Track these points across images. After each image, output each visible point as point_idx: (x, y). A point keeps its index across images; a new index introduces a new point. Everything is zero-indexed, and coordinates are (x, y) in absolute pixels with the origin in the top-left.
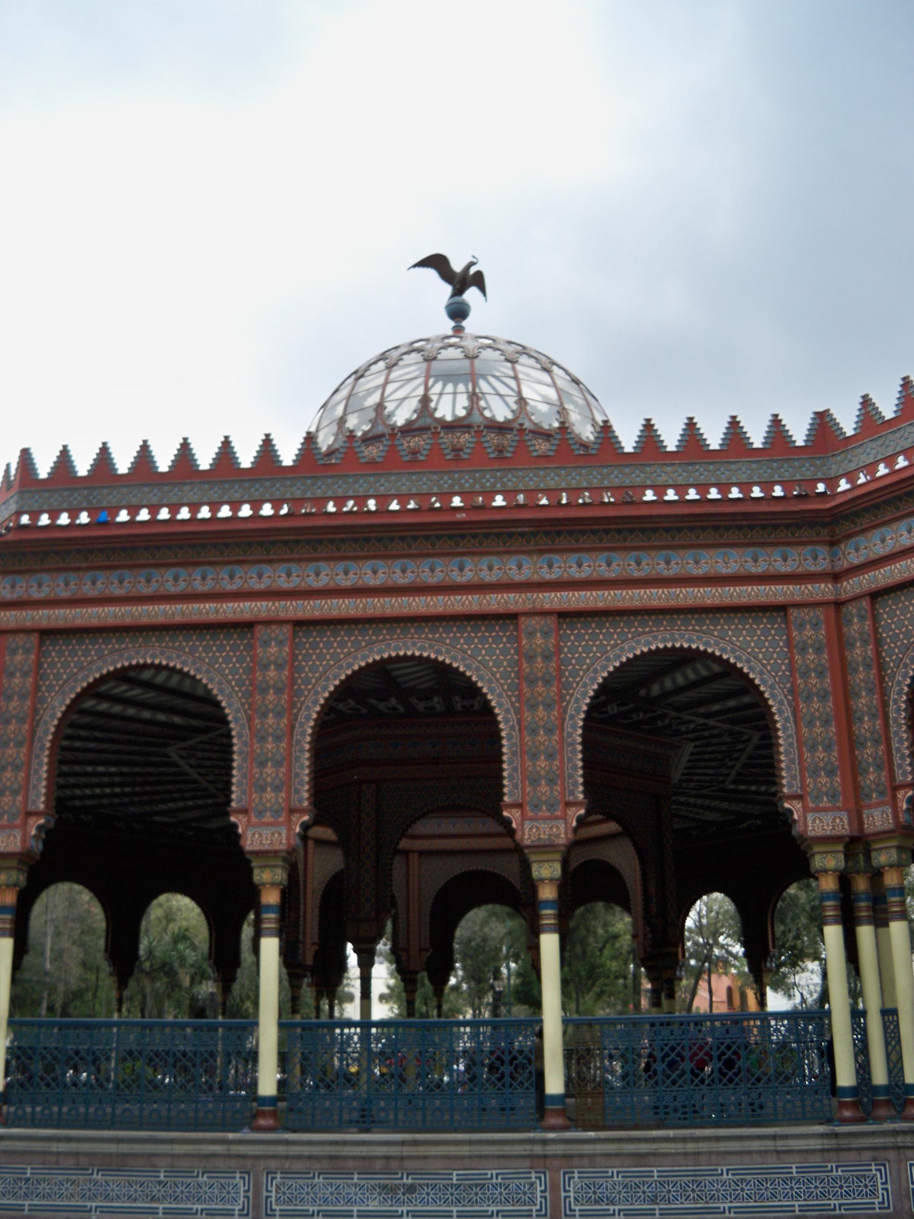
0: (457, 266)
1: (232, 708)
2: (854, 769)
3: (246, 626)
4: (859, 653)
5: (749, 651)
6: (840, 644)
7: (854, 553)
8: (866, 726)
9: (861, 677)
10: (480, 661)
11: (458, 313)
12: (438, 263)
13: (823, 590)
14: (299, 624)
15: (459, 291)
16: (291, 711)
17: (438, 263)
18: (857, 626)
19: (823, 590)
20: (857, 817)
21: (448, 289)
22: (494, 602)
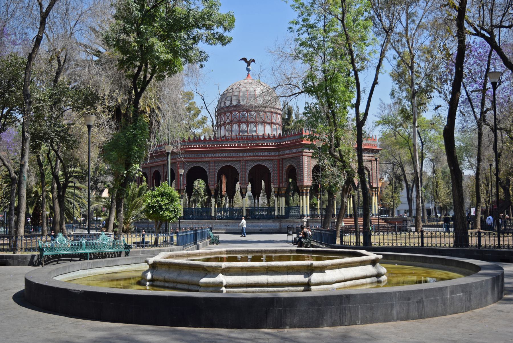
0: (248, 60)
1: (207, 171)
2: (279, 180)
3: (208, 162)
4: (281, 165)
5: (269, 165)
6: (279, 164)
7: (281, 153)
8: (281, 175)
9: (281, 168)
10: (237, 166)
11: (248, 70)
12: (244, 59)
13: (277, 158)
14: (215, 161)
15: (249, 65)
16: (214, 172)
17: (244, 59)
18: (281, 162)
19: (277, 158)
20: (279, 185)
21: (247, 64)
22: (238, 159)
